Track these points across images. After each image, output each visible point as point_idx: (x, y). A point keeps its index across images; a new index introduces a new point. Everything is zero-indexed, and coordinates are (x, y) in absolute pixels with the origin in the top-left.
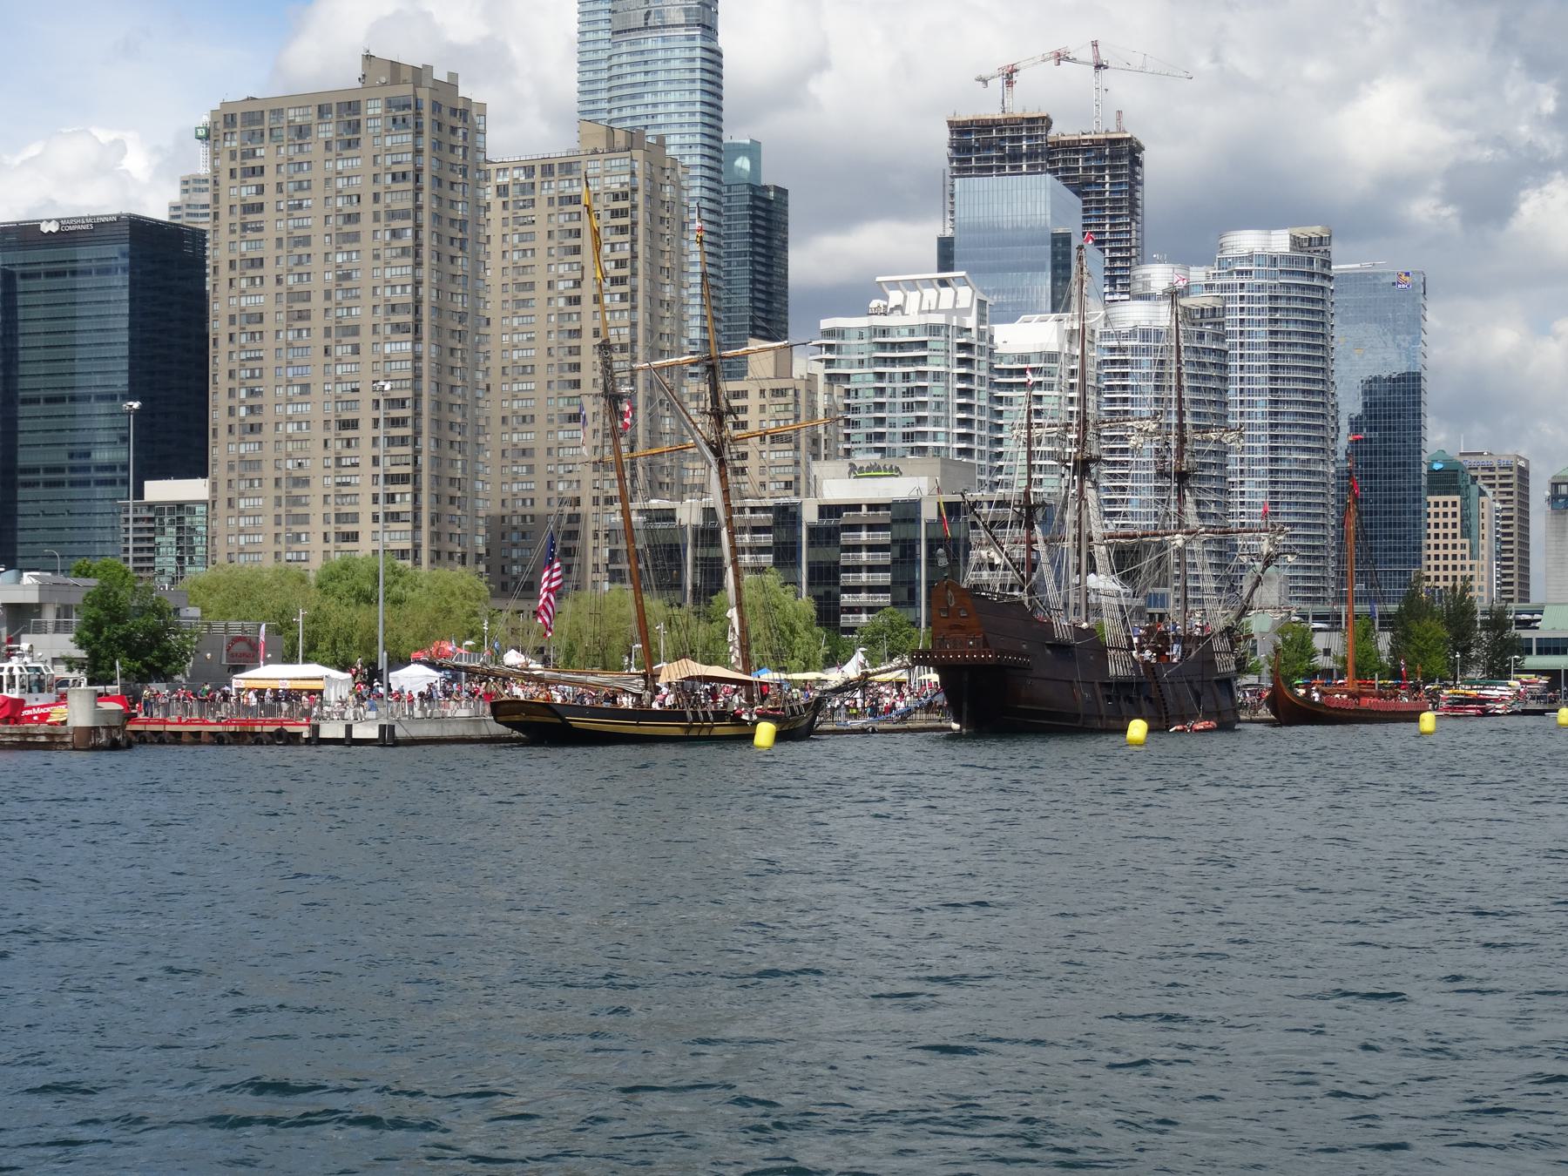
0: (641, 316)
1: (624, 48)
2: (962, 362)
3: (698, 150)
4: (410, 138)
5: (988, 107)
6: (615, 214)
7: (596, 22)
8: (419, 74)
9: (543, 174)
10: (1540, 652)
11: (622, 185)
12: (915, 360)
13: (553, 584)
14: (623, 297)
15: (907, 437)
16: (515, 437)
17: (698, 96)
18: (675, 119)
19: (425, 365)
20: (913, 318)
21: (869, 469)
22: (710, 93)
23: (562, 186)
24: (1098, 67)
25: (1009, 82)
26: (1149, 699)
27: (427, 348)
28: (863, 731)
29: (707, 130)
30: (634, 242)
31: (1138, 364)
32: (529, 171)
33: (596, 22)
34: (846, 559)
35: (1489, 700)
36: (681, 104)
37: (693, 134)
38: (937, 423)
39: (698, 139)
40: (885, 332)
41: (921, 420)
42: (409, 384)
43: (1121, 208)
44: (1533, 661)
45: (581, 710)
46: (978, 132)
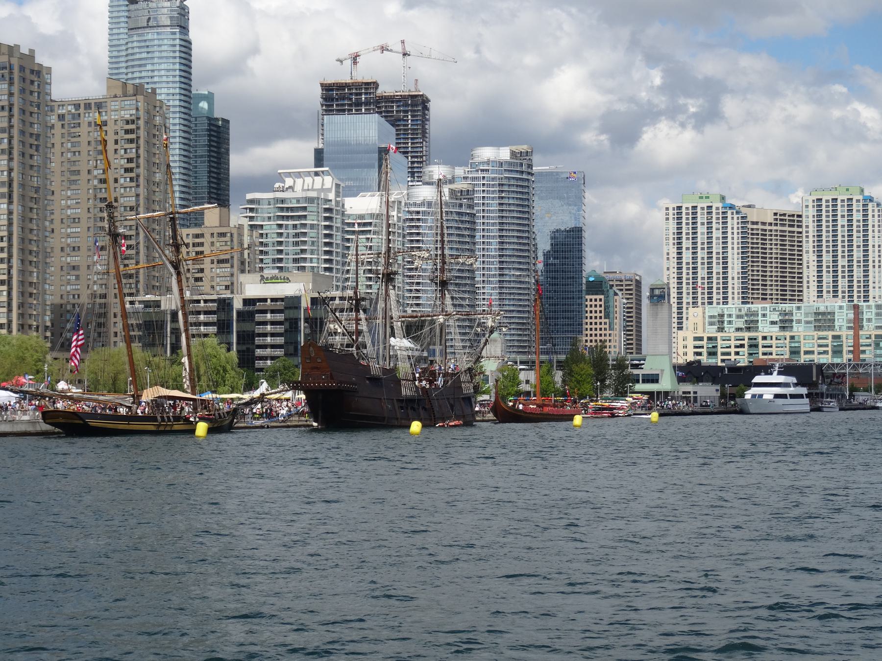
0: (142, 190)
1: (135, 38)
2: (327, 219)
3: (178, 97)
4: (6, 86)
5: (342, 75)
6: (127, 132)
7: (119, 23)
8: (12, 50)
9: (85, 108)
10: (644, 382)
11: (131, 115)
12: (300, 217)
13: (79, 343)
14: (131, 179)
15: (296, 261)
16: (69, 259)
17: (177, 67)
18: (165, 79)
19: (15, 217)
20: (299, 193)
21: (272, 278)
22: (184, 65)
23: (94, 116)
24: (405, 54)
25: (355, 62)
26: (424, 408)
27: (15, 207)
28: (262, 427)
29: (183, 86)
30: (138, 148)
31: (425, 221)
32: (77, 106)
33: (119, 23)
34: (259, 329)
35: (615, 409)
36: (168, 70)
37: (175, 88)
38: (312, 253)
39: (177, 91)
40: (283, 201)
41: (303, 251)
42: (5, 228)
43: (417, 134)
44: (640, 387)
45: (94, 415)
46: (337, 90)
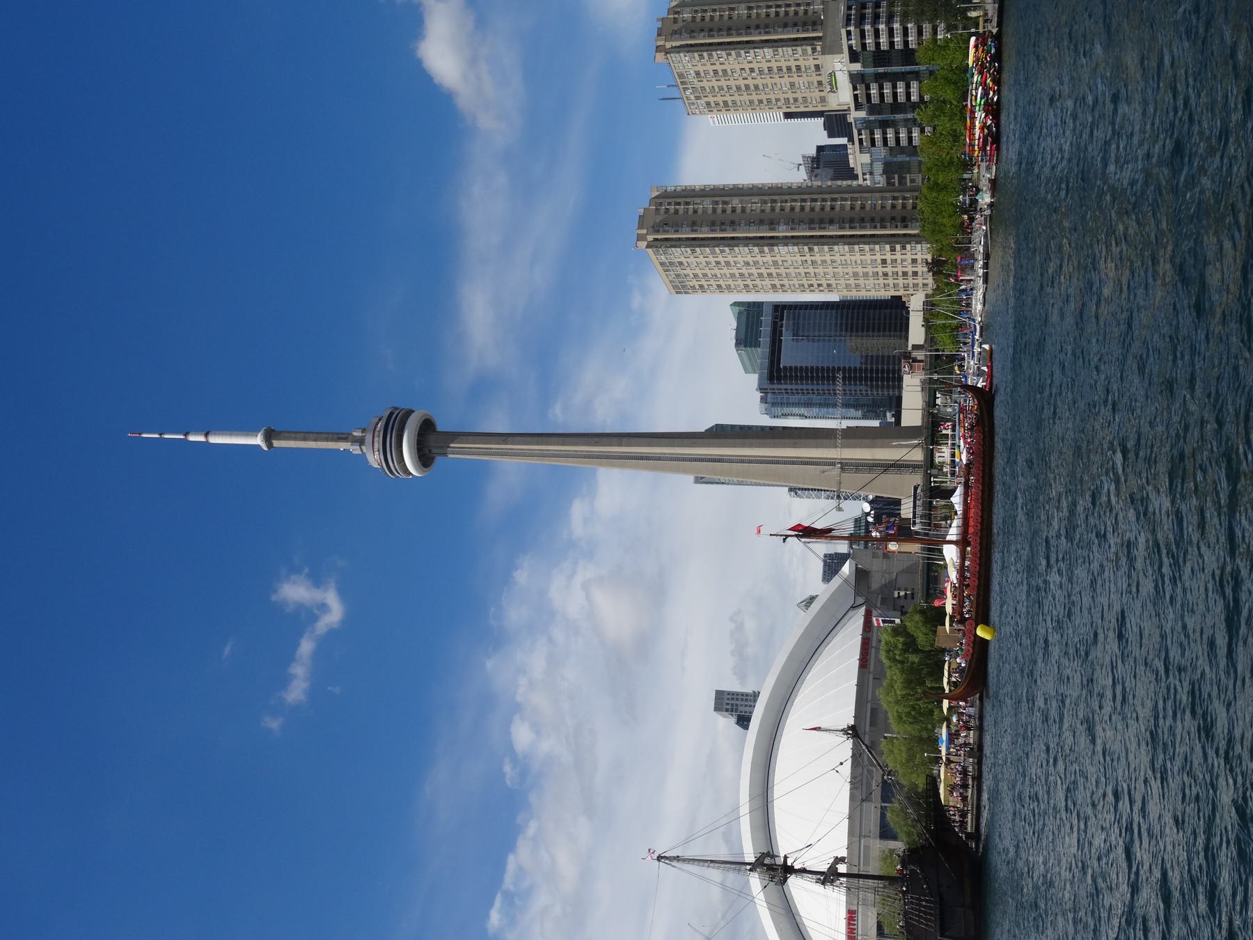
23: (691, 77)
